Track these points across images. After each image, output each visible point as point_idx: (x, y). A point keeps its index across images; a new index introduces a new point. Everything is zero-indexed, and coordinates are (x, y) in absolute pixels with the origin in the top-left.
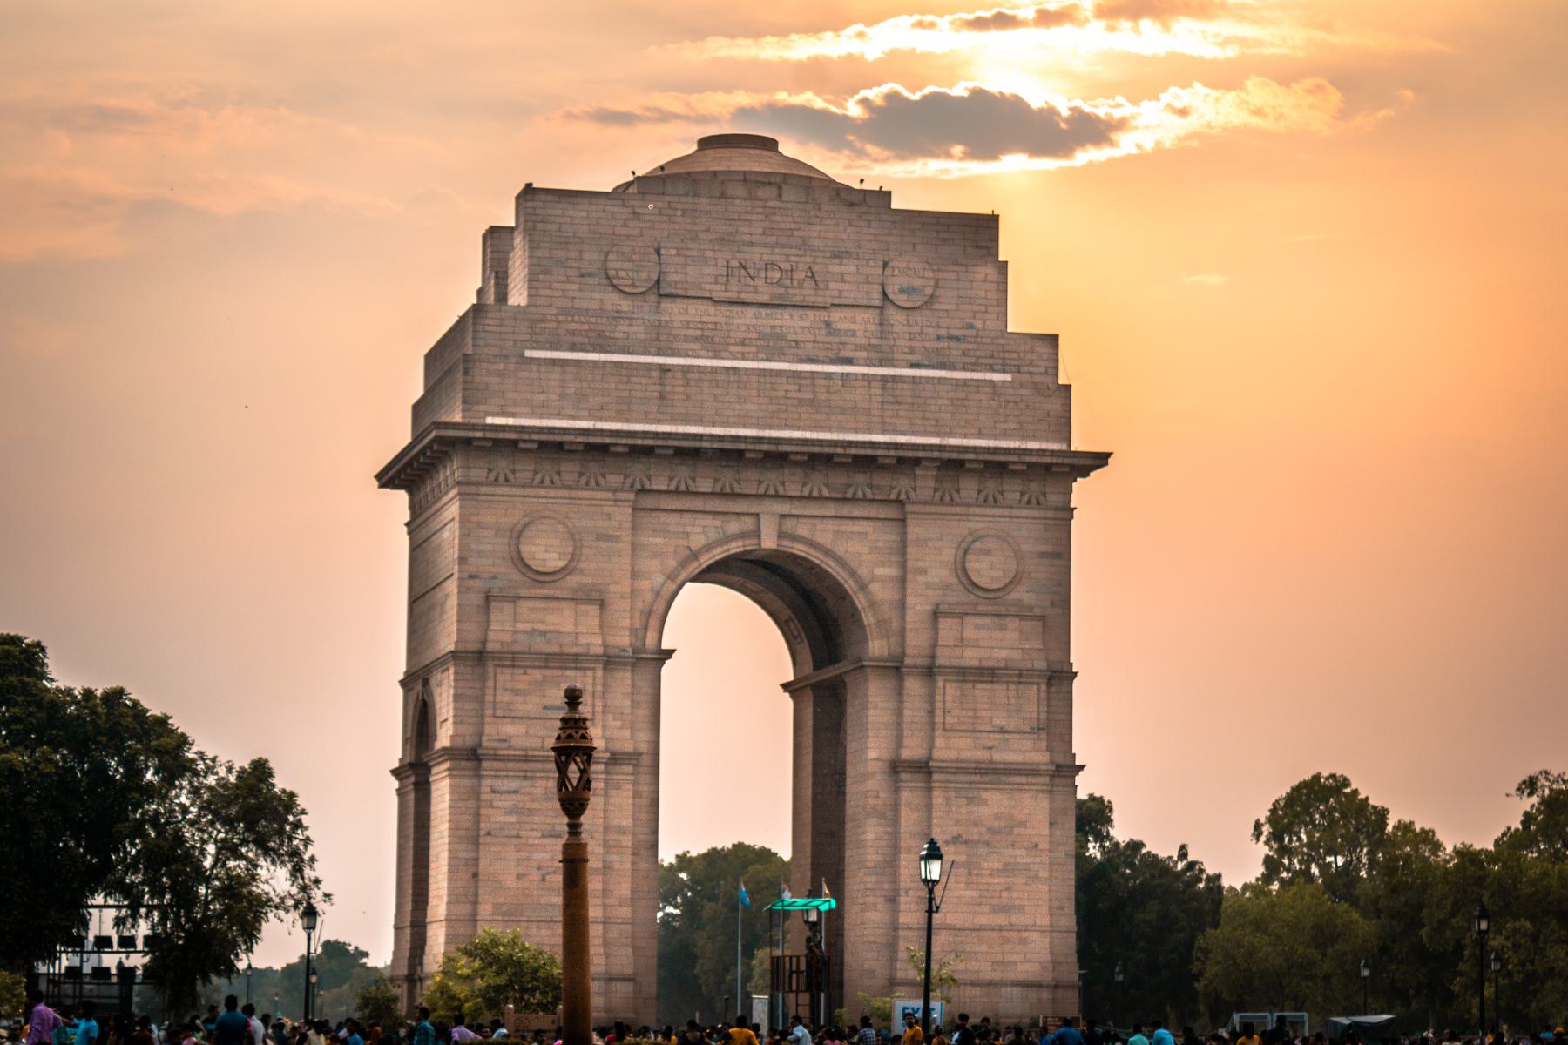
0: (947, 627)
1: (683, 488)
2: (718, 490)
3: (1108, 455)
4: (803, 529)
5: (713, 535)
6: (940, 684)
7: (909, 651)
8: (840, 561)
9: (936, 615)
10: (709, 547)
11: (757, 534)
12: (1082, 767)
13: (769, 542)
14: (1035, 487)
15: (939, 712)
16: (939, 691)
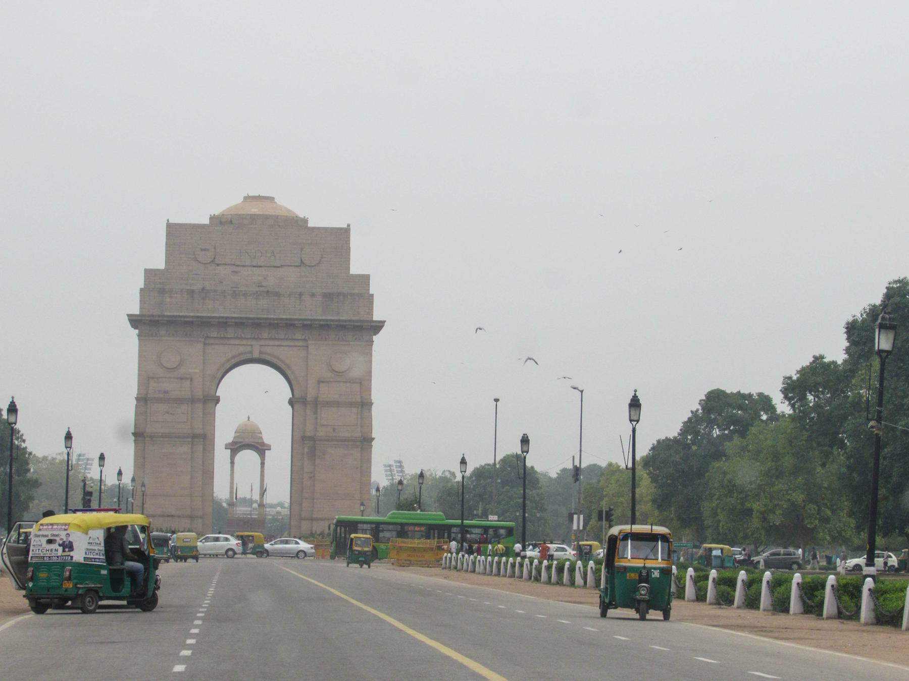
3: (384, 322)
8: (284, 362)
9: (319, 382)
11: (251, 352)
13: (256, 355)
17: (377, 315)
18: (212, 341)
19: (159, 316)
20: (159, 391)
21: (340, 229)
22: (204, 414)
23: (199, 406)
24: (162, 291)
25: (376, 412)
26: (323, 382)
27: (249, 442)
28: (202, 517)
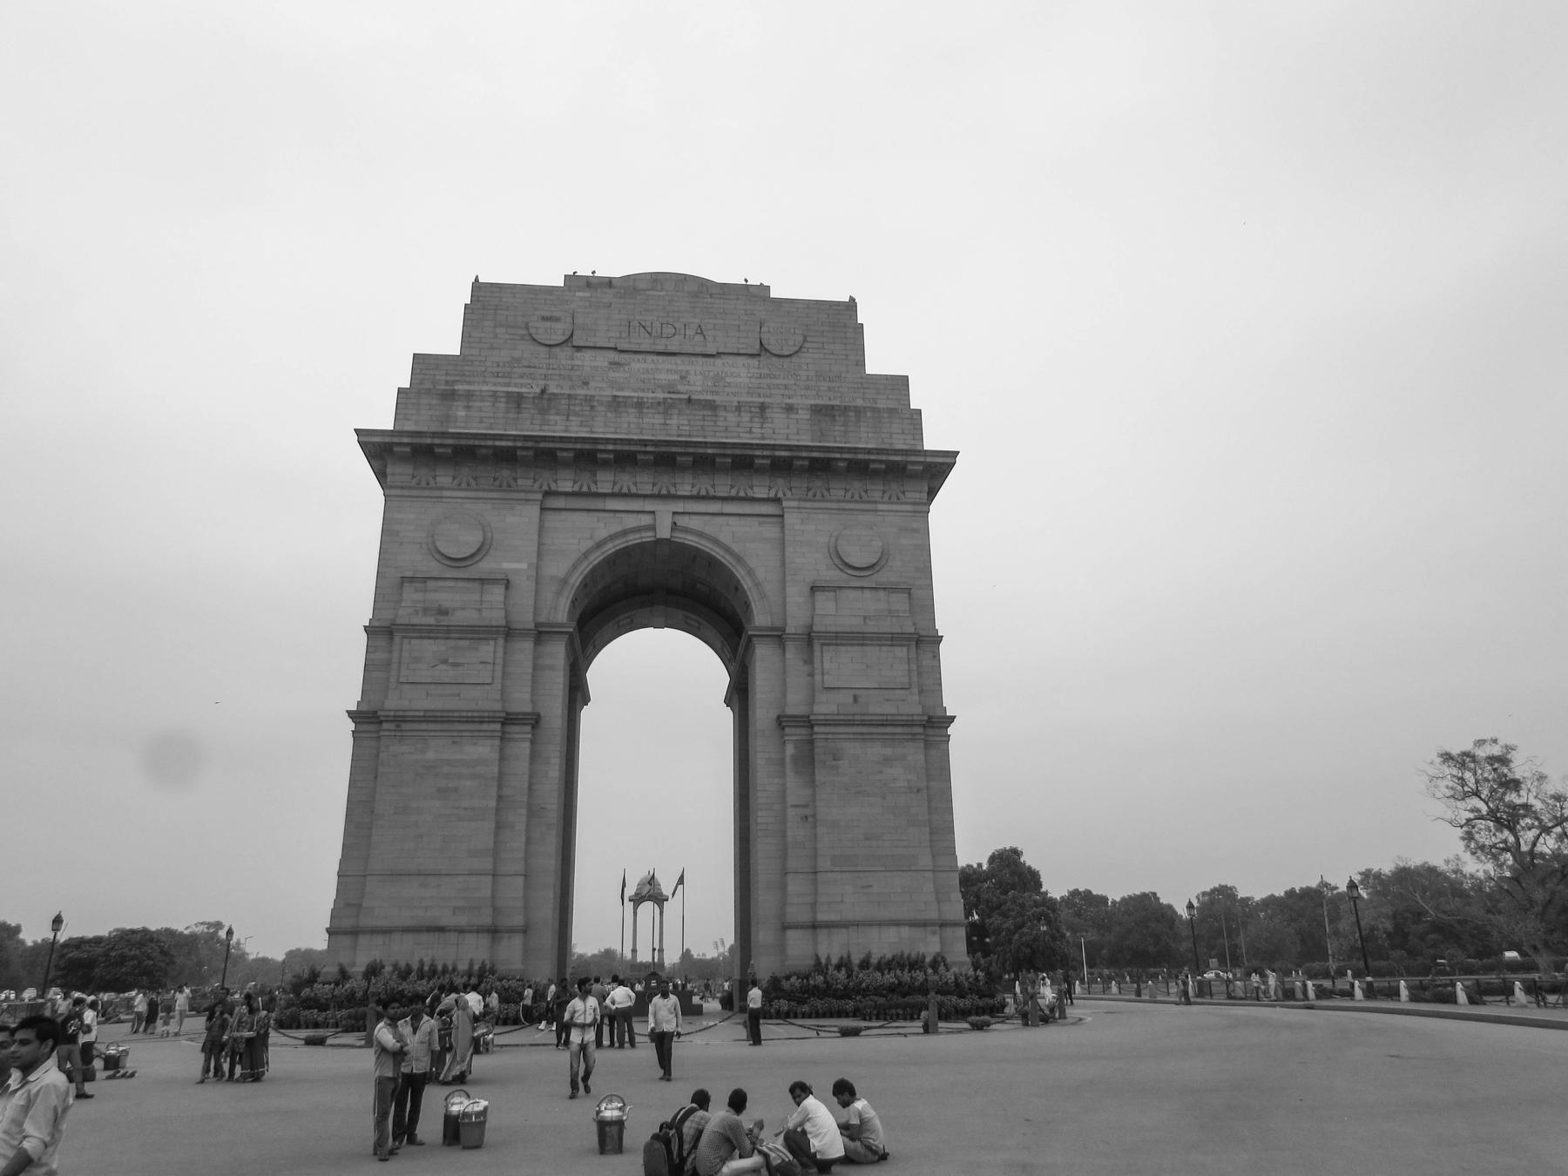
0: (825, 603)
1: (585, 489)
2: (616, 490)
4: (694, 523)
5: (615, 528)
6: (817, 647)
7: (789, 621)
8: (728, 550)
9: (814, 589)
10: (612, 538)
11: (653, 528)
12: (953, 718)
13: (664, 532)
14: (894, 486)
15: (818, 671)
16: (817, 654)
17: (934, 439)
18: (559, 503)
19: (434, 435)
20: (425, 610)
21: (838, 303)
22: (535, 668)
23: (528, 645)
24: (449, 396)
25: (952, 659)
26: (823, 589)
27: (650, 893)
28: (525, 931)
